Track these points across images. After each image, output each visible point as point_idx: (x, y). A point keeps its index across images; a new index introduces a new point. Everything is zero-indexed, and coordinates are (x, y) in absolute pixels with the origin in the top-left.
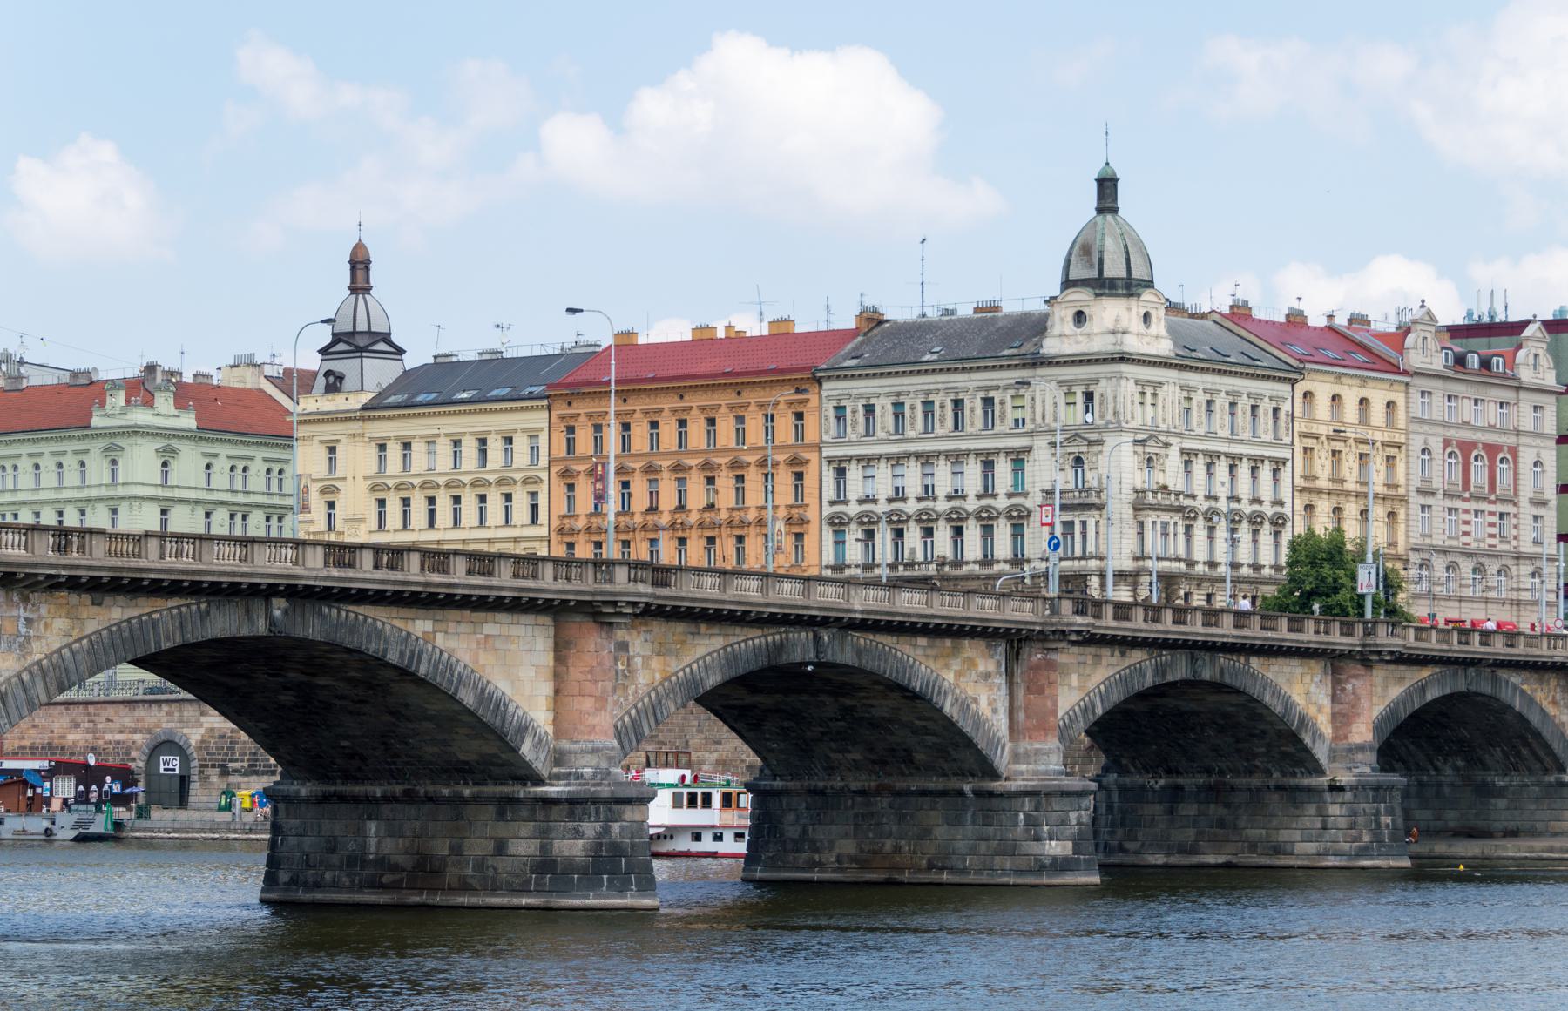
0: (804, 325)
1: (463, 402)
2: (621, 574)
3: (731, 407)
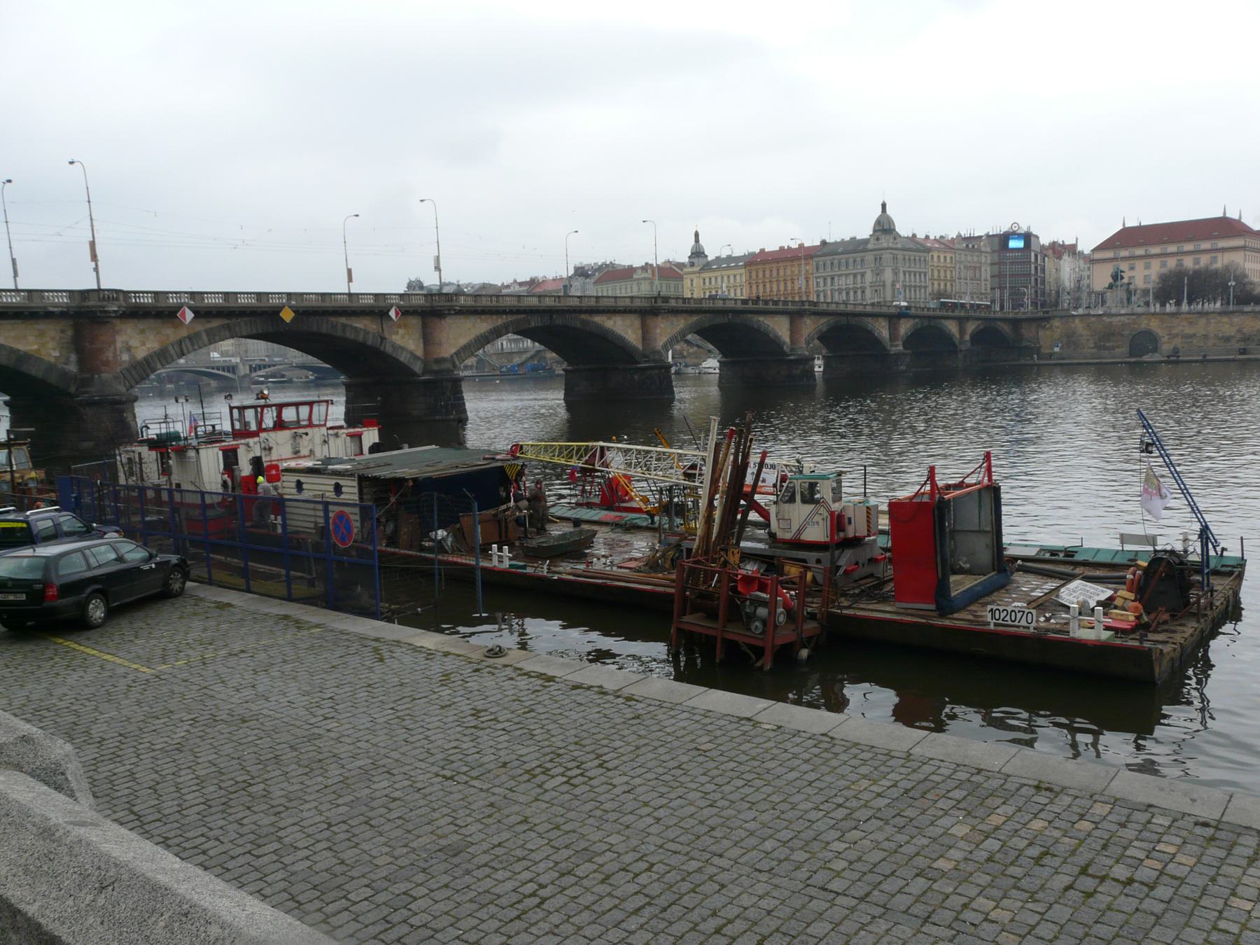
0: (858, 238)
2: (807, 304)
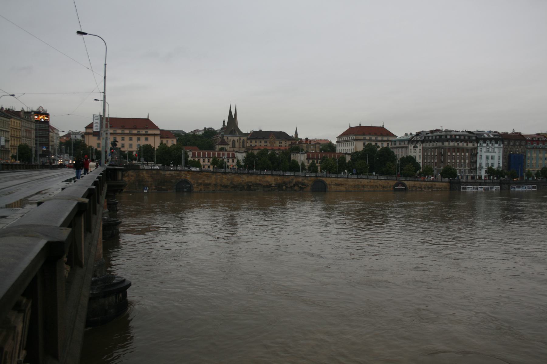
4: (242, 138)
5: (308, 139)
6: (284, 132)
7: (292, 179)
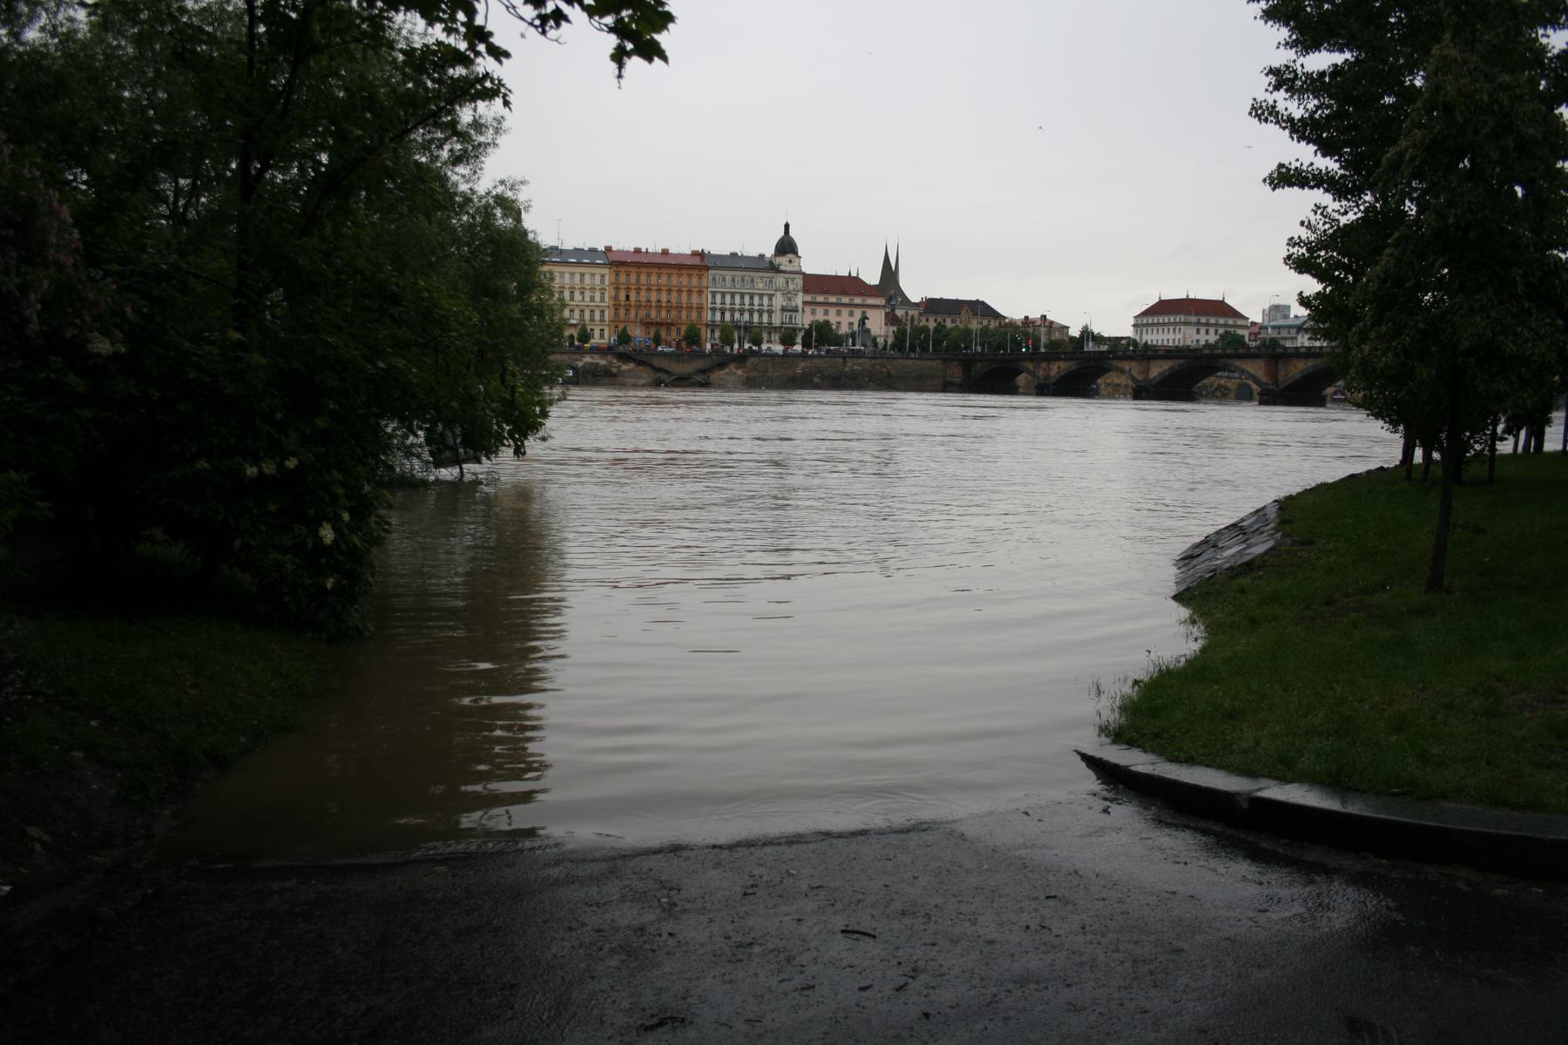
1: (572, 263)
3: (657, 273)
4: (911, 313)
5: (1047, 317)
6: (983, 303)
7: (1214, 382)
